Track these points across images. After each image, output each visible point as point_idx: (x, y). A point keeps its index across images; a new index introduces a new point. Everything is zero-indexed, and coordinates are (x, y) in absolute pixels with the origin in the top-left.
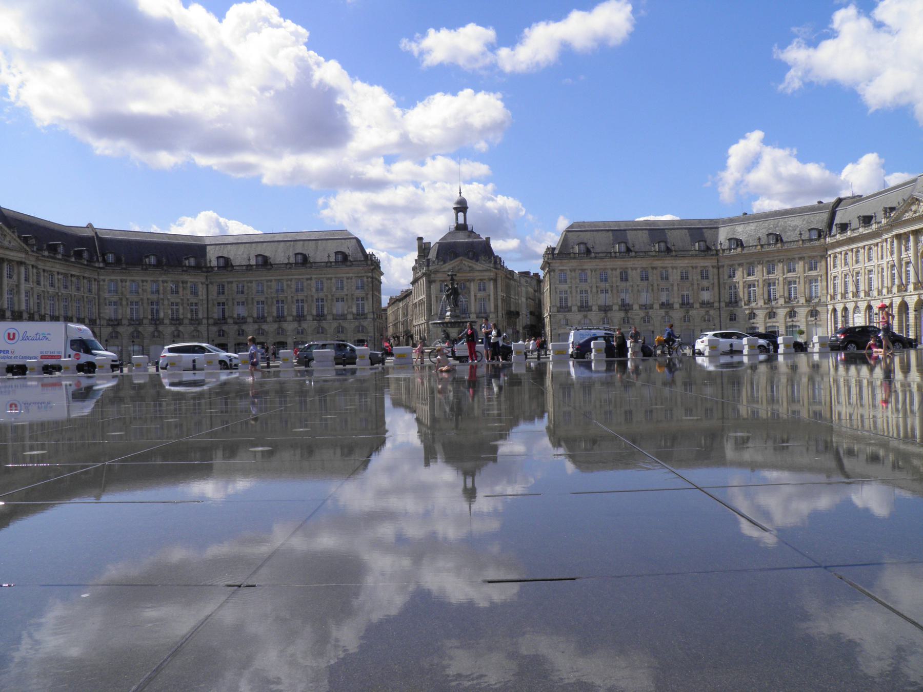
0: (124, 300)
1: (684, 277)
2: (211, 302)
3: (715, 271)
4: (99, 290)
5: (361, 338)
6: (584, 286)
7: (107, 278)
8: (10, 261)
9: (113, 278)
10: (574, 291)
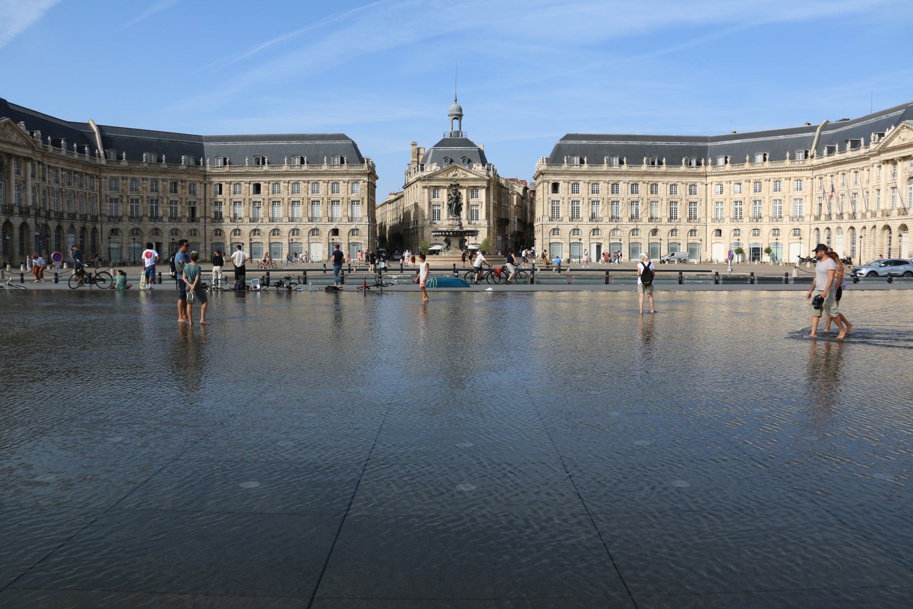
0: (125, 197)
2: (208, 201)
4: (100, 187)
6: (575, 197)
7: (109, 175)
8: (18, 157)
9: (114, 175)
10: (566, 200)
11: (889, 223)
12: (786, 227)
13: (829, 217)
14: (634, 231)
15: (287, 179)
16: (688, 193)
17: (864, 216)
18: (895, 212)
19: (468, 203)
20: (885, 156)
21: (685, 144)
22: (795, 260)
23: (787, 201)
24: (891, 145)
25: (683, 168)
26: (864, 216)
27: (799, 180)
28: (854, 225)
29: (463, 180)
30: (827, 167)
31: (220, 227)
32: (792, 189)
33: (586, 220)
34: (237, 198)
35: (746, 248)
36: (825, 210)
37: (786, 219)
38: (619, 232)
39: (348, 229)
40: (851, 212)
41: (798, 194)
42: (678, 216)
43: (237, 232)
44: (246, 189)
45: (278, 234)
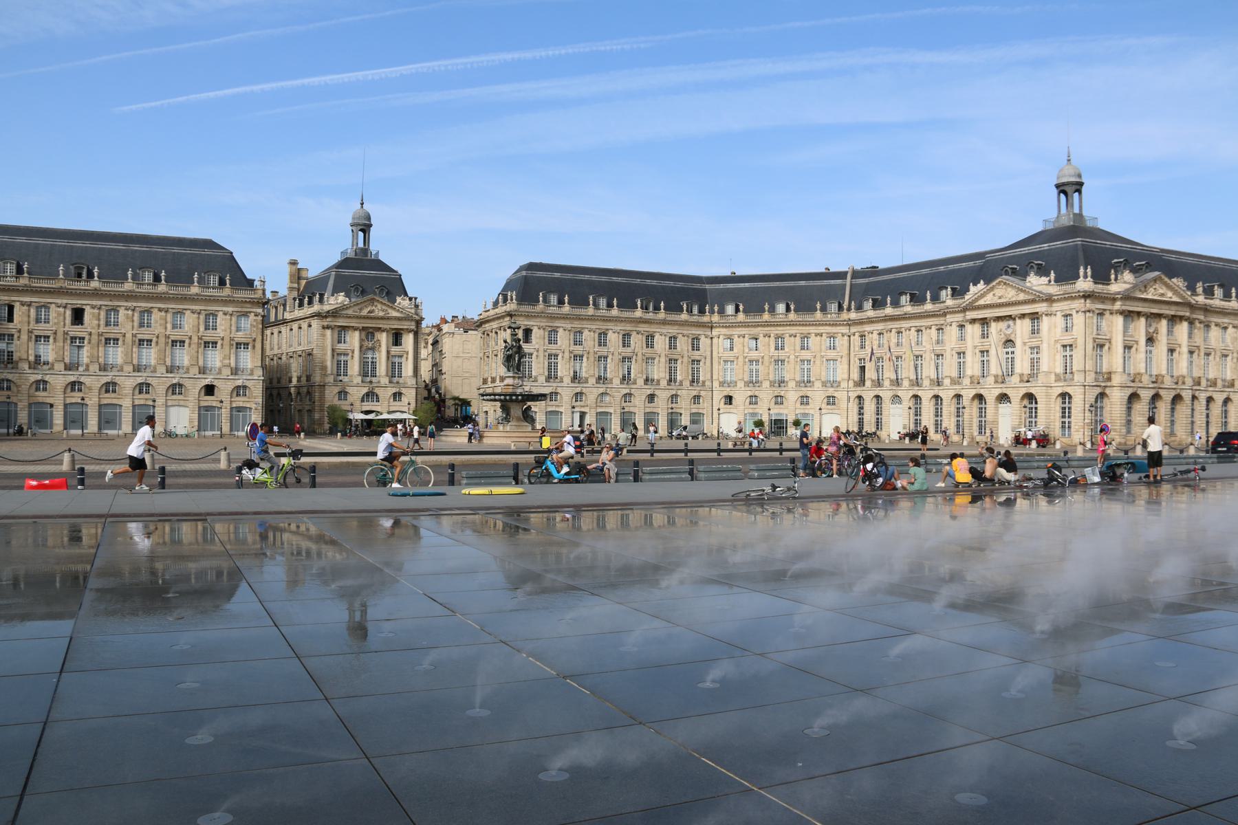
1: (672, 346)
3: (709, 341)
5: (241, 404)
10: (541, 354)
12: (818, 395)
13: (878, 383)
14: (628, 397)
15: (129, 304)
18: (991, 380)
19: (388, 352)
20: (971, 315)
21: (680, 284)
22: (896, 437)
23: (818, 362)
24: (981, 302)
27: (832, 337)
28: (919, 393)
29: (382, 318)
31: (10, 377)
32: (823, 348)
33: (567, 380)
34: (42, 328)
36: (870, 374)
37: (818, 385)
38: (607, 399)
39: (230, 386)
40: (913, 377)
41: (832, 354)
42: (679, 378)
43: (41, 385)
44: (59, 316)
45: (114, 391)
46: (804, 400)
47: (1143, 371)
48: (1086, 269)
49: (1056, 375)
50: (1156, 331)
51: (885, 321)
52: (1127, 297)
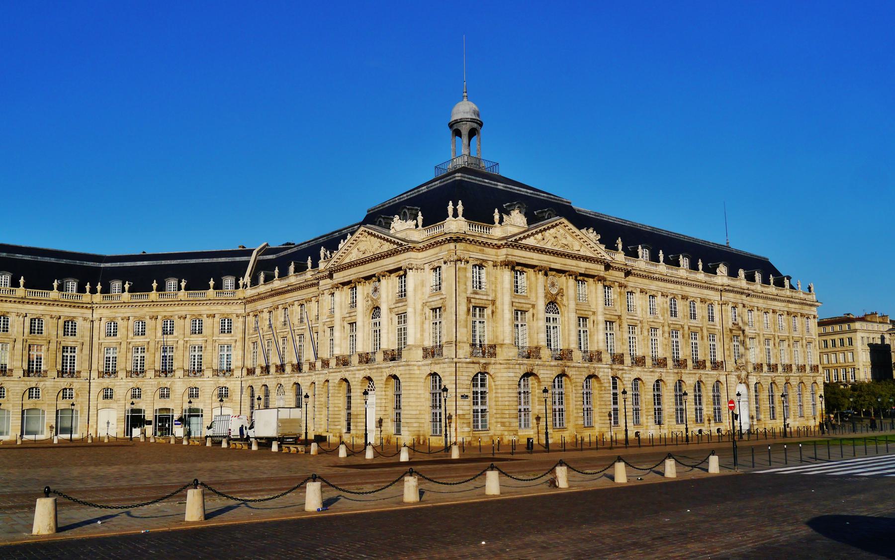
3: (88, 325)
11: (347, 375)
16: (61, 332)
17: (312, 366)
20: (339, 277)
21: (64, 261)
23: (209, 348)
24: (347, 260)
25: (54, 294)
26: (312, 366)
30: (262, 299)
35: (149, 416)
37: (208, 373)
40: (295, 362)
42: (43, 368)
46: (194, 393)
47: (543, 343)
48: (455, 205)
49: (425, 350)
50: (561, 292)
51: (272, 296)
52: (514, 243)
